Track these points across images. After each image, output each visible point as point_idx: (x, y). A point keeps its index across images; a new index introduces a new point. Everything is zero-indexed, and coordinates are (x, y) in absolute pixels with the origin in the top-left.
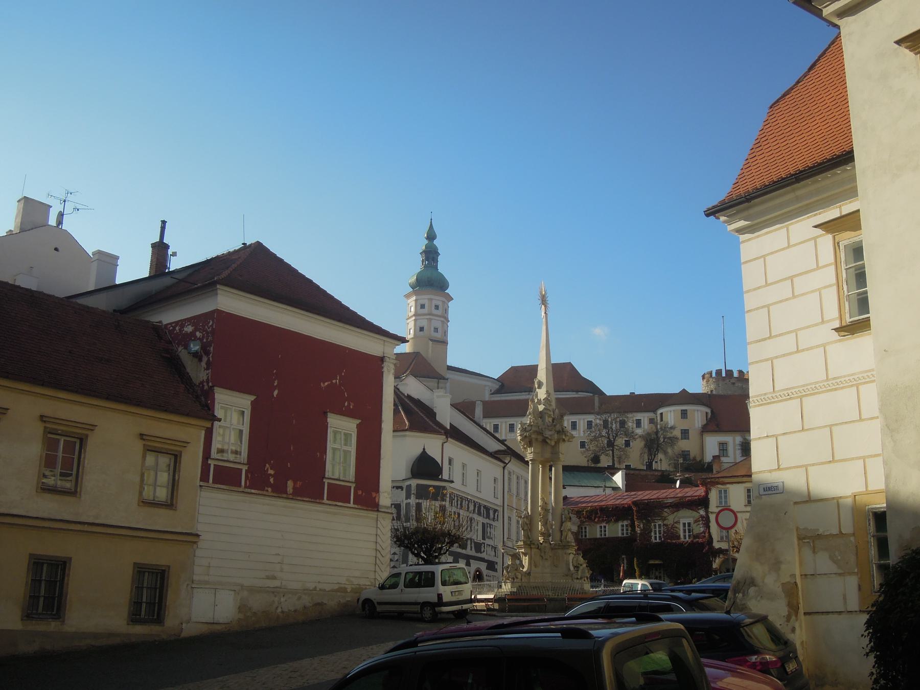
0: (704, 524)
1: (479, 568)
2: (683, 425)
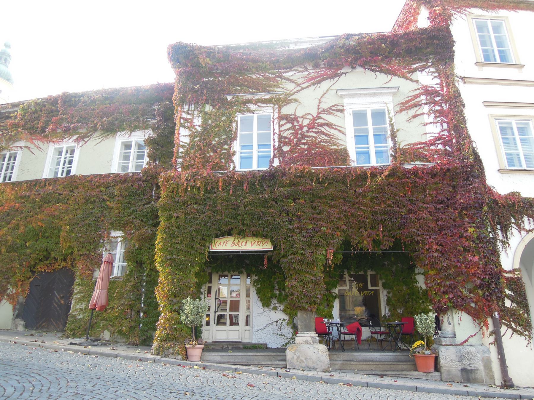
0: (441, 113)
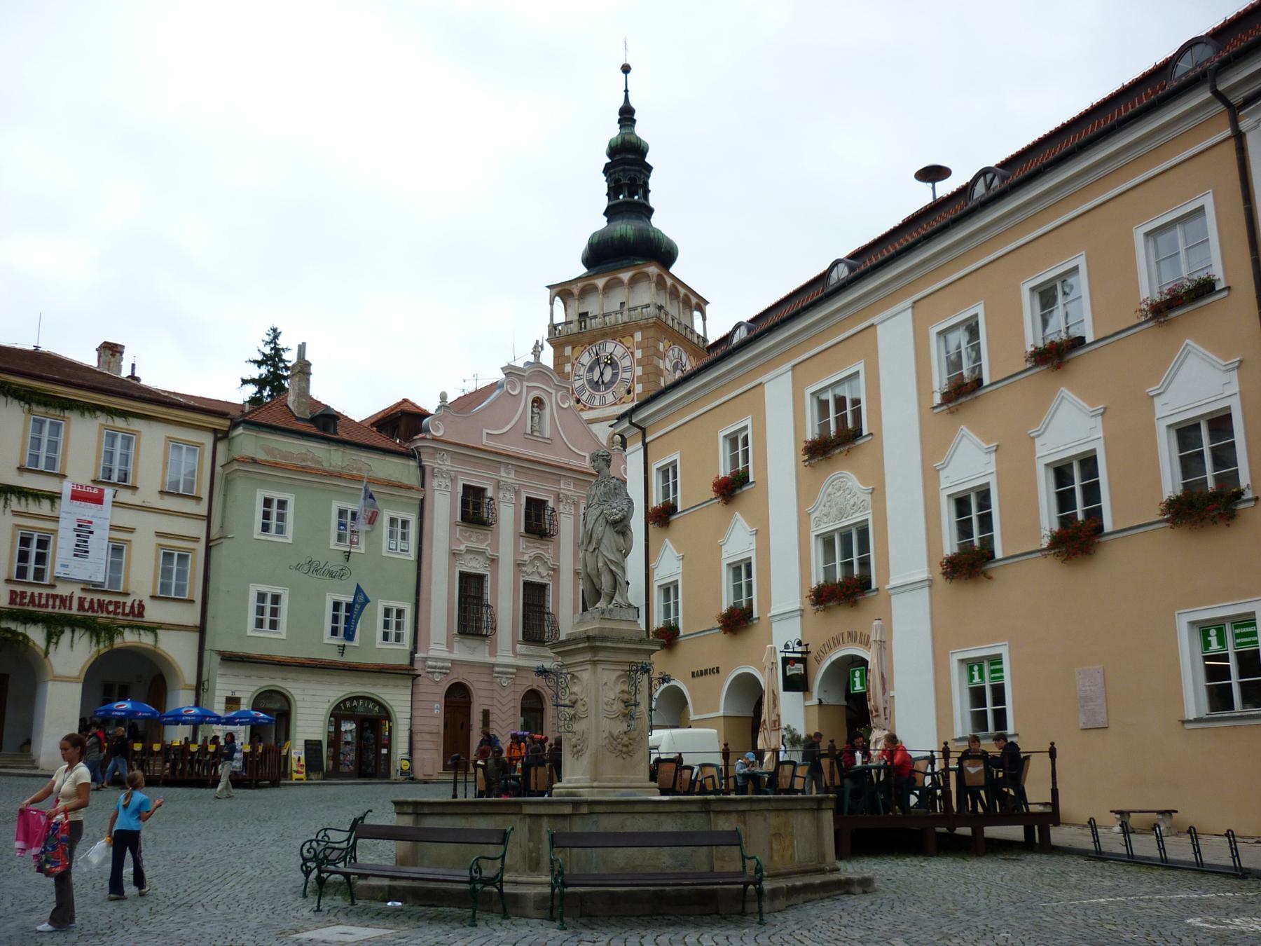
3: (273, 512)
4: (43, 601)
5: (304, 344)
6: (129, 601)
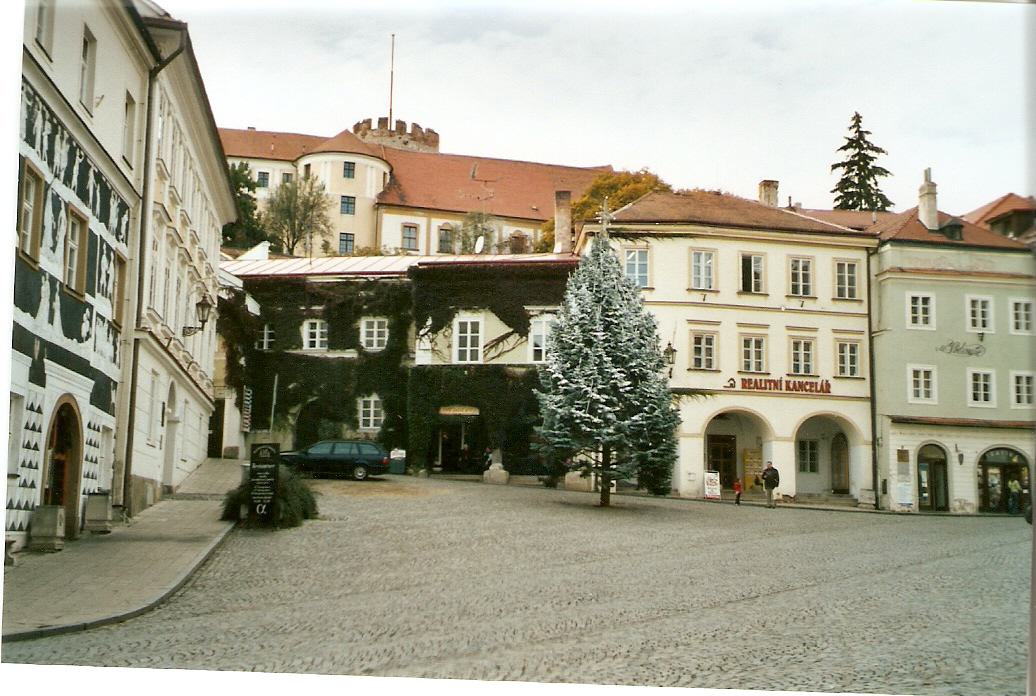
1: (70, 395)
2: (349, 188)
3: (920, 306)
4: (763, 386)
5: (929, 169)
6: (819, 381)
